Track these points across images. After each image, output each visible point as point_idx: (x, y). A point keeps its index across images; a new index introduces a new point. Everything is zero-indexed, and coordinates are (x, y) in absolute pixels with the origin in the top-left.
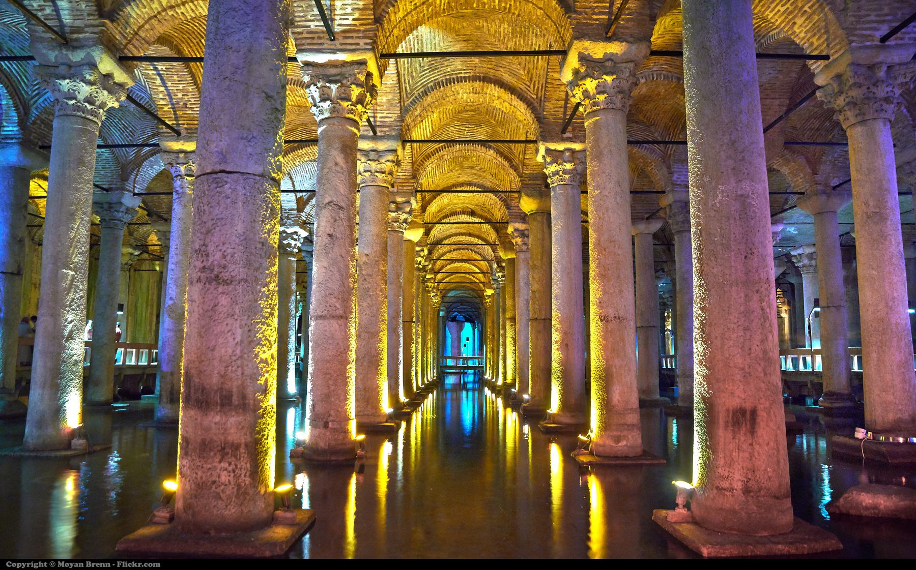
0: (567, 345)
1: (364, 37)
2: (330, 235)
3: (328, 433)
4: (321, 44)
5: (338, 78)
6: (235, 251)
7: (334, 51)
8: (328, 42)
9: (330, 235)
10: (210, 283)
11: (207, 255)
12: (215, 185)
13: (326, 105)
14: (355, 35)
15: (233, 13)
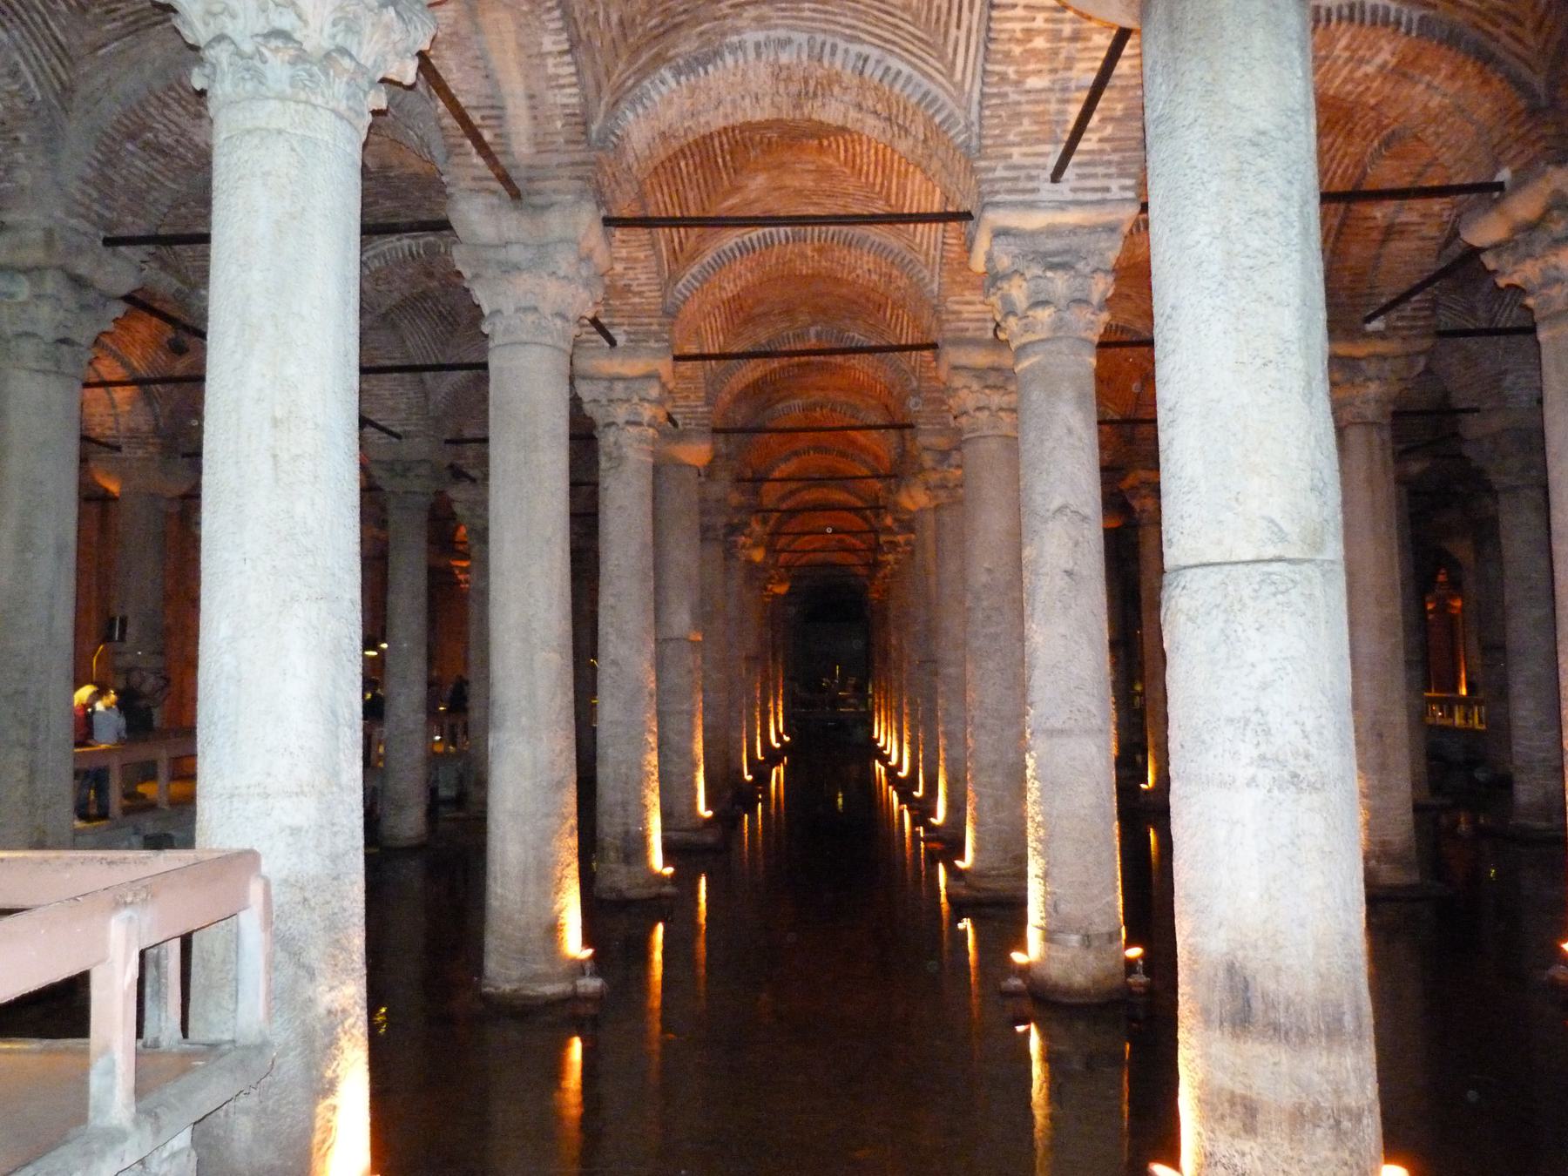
0: (1380, 735)
1: (1121, 176)
2: (1069, 573)
3: (1091, 957)
4: (1034, 191)
5: (1066, 258)
6: (1323, 720)
7: (1062, 206)
8: (1049, 185)
9: (1069, 573)
10: (1280, 788)
11: (1267, 732)
12: (1273, 589)
13: (1044, 314)
14: (1100, 170)
15: (1262, 221)
